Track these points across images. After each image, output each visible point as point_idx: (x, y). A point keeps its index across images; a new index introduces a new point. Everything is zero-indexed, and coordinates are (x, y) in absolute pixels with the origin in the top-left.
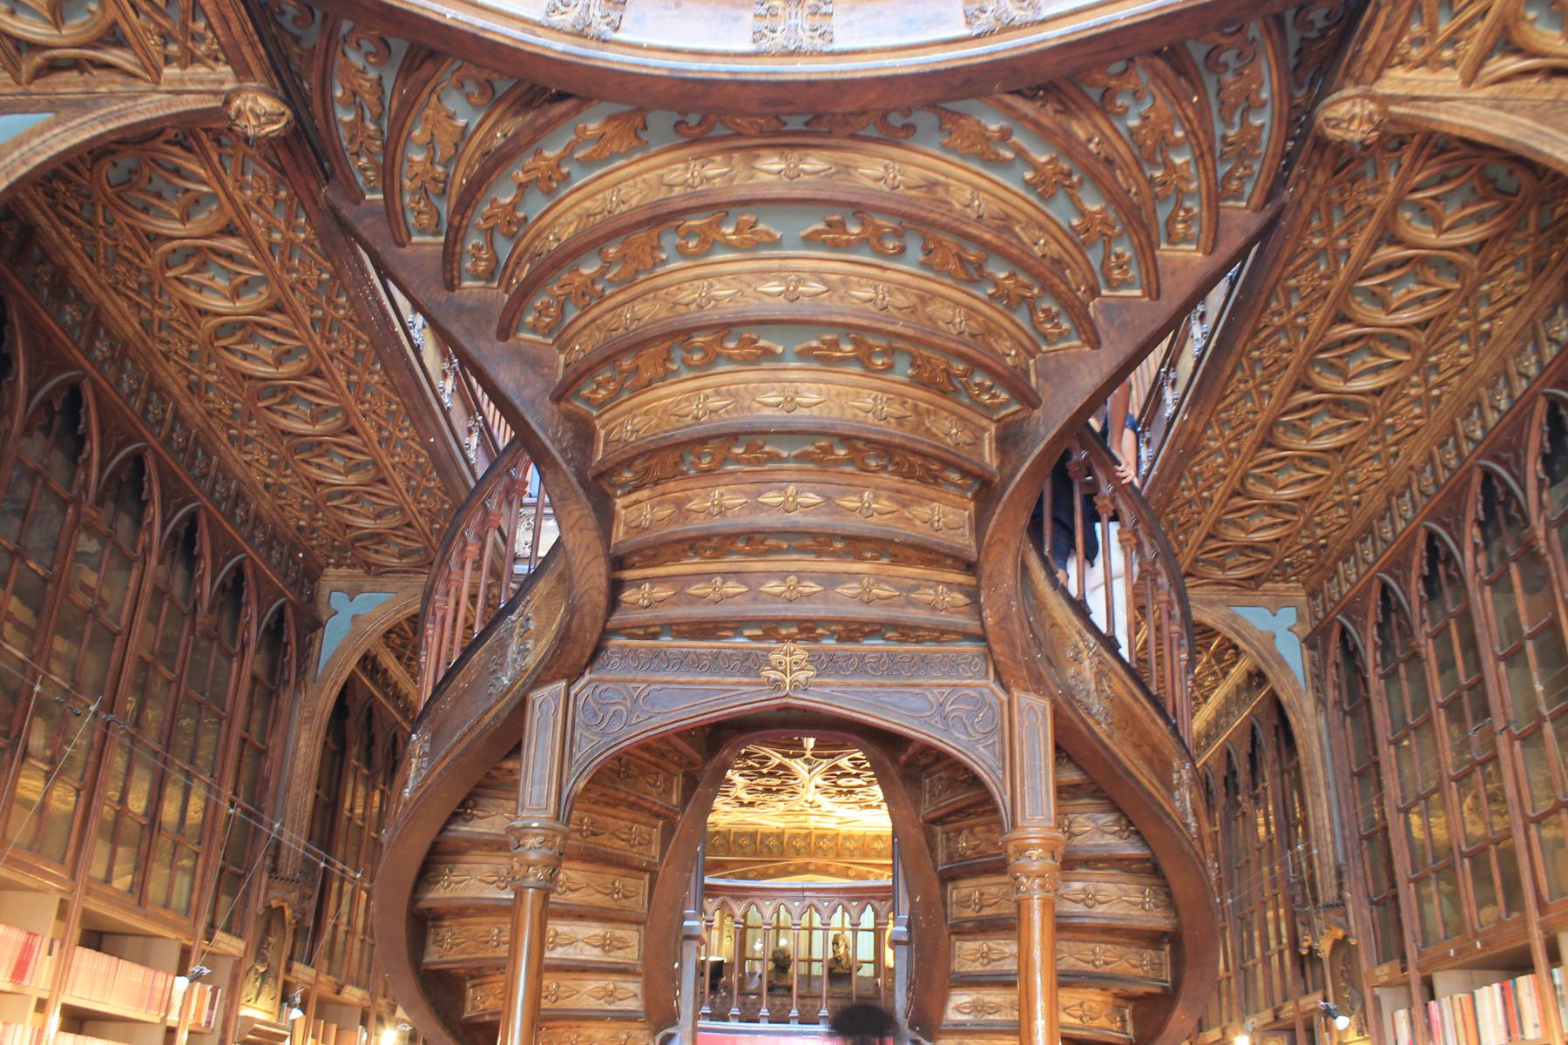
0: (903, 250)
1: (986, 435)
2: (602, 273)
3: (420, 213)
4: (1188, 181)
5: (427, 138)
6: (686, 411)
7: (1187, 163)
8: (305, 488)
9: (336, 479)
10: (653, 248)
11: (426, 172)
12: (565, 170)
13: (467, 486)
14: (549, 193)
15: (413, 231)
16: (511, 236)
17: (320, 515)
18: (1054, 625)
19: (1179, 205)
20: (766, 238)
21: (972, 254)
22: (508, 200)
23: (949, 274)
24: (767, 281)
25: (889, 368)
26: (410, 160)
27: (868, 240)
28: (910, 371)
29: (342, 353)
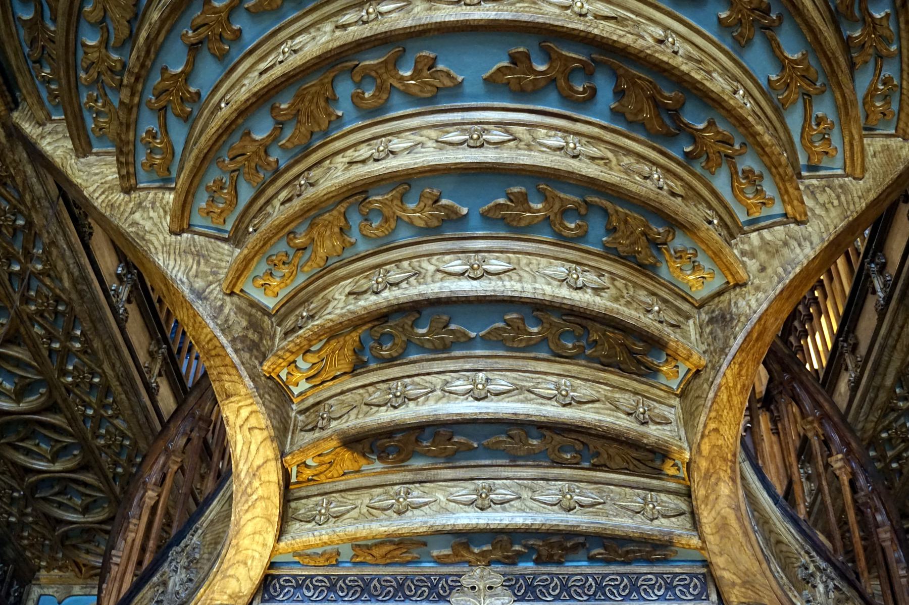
0: (592, 93)
1: (691, 322)
2: (274, 138)
3: (99, 113)
4: (889, 43)
5: (98, 15)
6: (365, 287)
7: (887, 15)
8: (13, 477)
9: (40, 465)
10: (327, 100)
11: (101, 60)
12: (236, 27)
13: (152, 430)
14: (221, 57)
15: (94, 141)
16: (186, 118)
17: (29, 510)
18: (779, 542)
19: (878, 70)
20: (447, 82)
21: (669, 95)
22: (180, 70)
23: (642, 126)
24: (448, 133)
25: (582, 237)
26: (84, 45)
27: (554, 80)
28: (604, 239)
29: (42, 316)
